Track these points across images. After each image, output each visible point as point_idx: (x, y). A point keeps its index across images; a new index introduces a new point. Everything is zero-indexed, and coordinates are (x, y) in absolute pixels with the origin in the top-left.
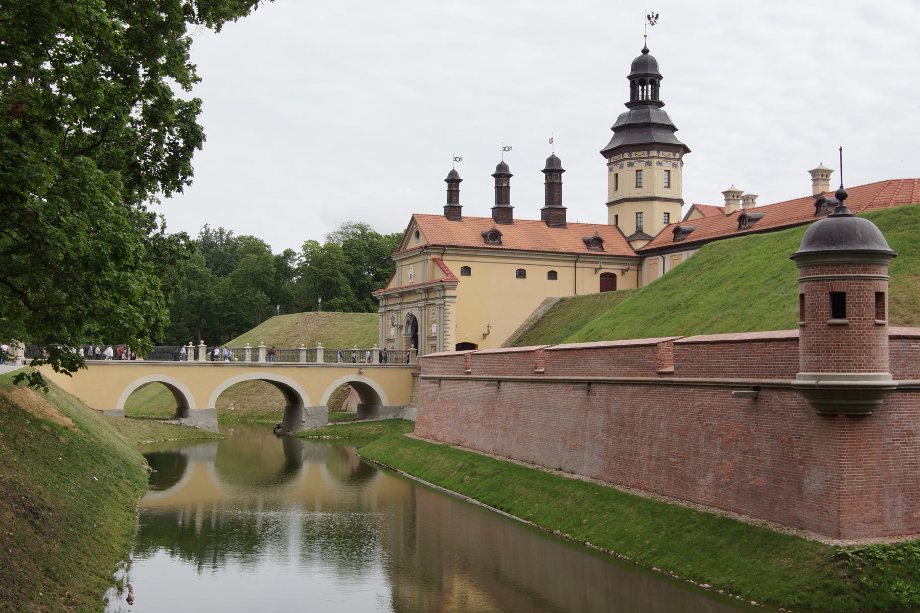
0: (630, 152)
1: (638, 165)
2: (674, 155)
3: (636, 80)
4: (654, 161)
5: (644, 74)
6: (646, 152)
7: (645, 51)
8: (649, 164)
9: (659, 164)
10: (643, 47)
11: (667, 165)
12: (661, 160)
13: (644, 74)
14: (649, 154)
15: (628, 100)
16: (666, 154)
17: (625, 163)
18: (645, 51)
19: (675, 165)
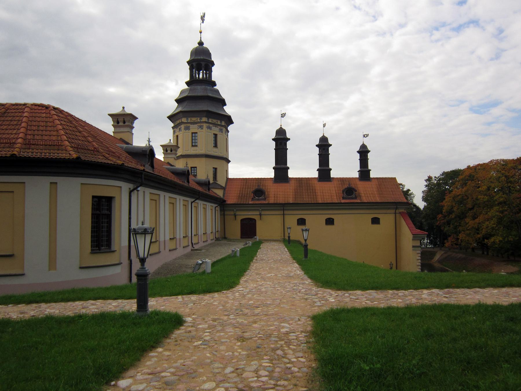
0: (187, 117)
1: (194, 128)
2: (221, 122)
3: (194, 64)
4: (205, 125)
5: (201, 61)
6: (199, 119)
7: (201, 43)
8: (201, 127)
9: (209, 128)
10: (199, 41)
11: (216, 130)
12: (211, 125)
13: (201, 61)
14: (201, 119)
15: (188, 79)
16: (215, 121)
17: (183, 126)
18: (201, 43)
19: (221, 130)
